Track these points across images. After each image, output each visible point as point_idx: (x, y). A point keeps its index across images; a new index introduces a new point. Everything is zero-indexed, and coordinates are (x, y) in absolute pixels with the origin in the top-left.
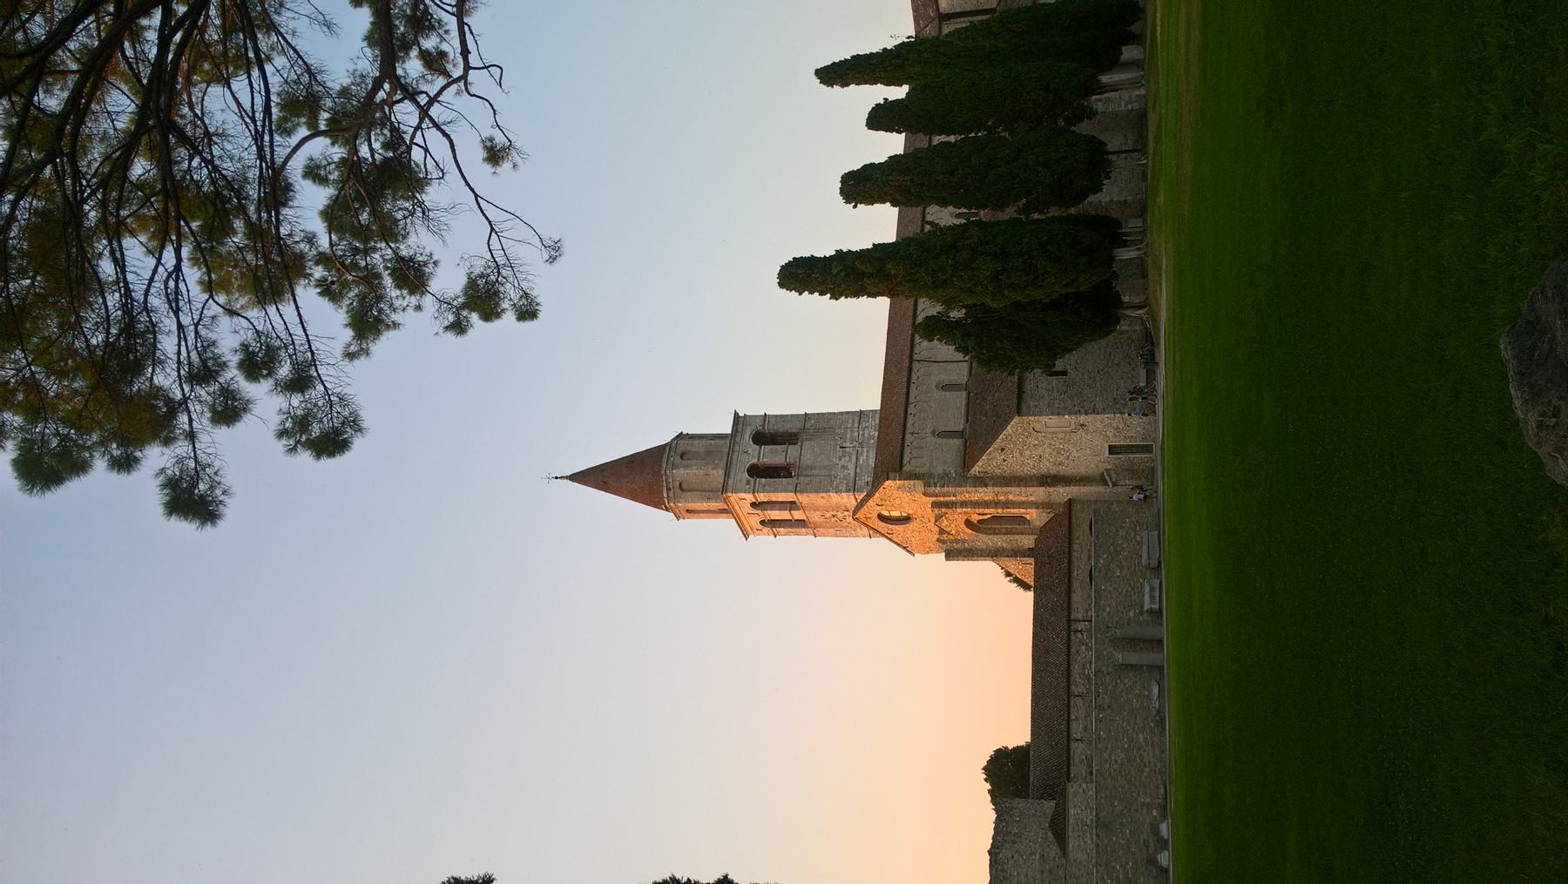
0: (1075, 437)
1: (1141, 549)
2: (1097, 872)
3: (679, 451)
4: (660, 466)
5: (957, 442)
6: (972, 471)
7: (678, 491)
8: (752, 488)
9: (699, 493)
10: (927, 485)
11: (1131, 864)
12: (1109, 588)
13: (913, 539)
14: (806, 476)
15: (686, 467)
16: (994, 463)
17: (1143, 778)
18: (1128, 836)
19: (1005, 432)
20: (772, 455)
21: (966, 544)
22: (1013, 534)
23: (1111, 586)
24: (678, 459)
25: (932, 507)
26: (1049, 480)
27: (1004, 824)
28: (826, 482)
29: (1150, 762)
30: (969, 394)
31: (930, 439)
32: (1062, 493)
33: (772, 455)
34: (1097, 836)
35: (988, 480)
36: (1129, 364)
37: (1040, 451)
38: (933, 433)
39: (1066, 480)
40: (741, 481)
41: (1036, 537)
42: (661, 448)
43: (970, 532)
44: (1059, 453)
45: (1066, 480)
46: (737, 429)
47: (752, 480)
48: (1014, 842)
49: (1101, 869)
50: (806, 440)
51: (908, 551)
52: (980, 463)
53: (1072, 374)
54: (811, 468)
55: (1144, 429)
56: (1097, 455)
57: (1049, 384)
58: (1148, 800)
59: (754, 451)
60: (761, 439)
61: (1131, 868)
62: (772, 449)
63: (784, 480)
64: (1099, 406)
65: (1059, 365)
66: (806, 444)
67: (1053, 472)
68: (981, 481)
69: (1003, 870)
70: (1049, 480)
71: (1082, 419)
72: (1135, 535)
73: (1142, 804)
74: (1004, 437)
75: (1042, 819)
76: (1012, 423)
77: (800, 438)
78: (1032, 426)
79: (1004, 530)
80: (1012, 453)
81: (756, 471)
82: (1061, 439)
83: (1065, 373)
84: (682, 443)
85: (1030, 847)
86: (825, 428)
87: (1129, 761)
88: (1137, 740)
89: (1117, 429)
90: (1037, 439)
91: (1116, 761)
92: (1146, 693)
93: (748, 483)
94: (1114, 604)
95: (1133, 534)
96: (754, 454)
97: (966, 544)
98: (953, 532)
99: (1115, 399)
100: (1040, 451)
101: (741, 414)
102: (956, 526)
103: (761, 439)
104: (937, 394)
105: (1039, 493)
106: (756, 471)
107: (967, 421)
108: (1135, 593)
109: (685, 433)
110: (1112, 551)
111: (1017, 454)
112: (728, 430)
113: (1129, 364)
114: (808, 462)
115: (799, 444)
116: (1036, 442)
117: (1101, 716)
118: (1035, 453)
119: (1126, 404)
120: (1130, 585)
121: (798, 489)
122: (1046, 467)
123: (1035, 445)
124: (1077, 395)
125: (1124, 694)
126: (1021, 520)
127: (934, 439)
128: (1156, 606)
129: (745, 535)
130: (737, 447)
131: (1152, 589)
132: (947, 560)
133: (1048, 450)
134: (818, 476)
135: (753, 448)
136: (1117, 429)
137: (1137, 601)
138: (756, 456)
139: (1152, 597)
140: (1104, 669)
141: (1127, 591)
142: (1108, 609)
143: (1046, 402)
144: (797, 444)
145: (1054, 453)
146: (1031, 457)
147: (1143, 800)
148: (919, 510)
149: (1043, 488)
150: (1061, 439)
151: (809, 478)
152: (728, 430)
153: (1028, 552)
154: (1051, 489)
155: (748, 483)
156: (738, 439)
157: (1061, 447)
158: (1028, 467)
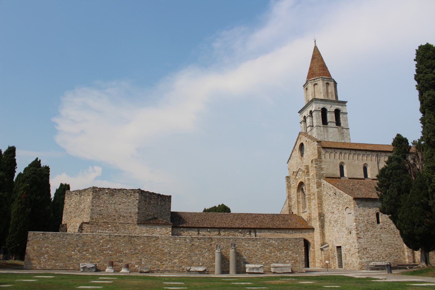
0: (344, 229)
1: (282, 263)
2: (107, 236)
3: (329, 82)
4: (323, 76)
5: (338, 174)
6: (324, 181)
7: (314, 83)
8: (317, 109)
9: (314, 91)
10: (316, 161)
11: (111, 252)
12: (258, 246)
13: (293, 161)
14: (324, 130)
15: (323, 85)
16: (328, 191)
17: (154, 261)
18: (124, 252)
19: (344, 193)
20: (331, 117)
21: (293, 185)
22: (298, 204)
23: (260, 247)
24: (326, 82)
25: (307, 165)
26: (322, 218)
27: (156, 197)
28: (322, 137)
29: (163, 265)
30: (364, 179)
31: (339, 162)
32: (316, 224)
33: (331, 117)
34: (125, 236)
35: (320, 189)
36: (386, 256)
37: (336, 212)
38: (342, 163)
39: (322, 227)
40: (319, 105)
41: (297, 215)
42: (330, 75)
43: (298, 185)
44: (336, 221)
45: (322, 227)
46: (340, 103)
47: (320, 109)
48: (145, 201)
49: (108, 238)
50: (338, 129)
51: (289, 160)
52: (328, 184)
53: (379, 226)
54: (327, 132)
55: (351, 264)
56: (336, 240)
57: (372, 214)
58: (143, 263)
59: (332, 109)
60: (337, 112)
61: (108, 253)
62: (333, 116)
63: (321, 121)
64: (361, 241)
65: (384, 218)
66: (337, 129)
67: (326, 219)
68: (319, 185)
69: (131, 195)
70: (322, 218)
71: (354, 232)
72: (289, 260)
73: (141, 260)
74: (342, 193)
75: (159, 214)
76: (349, 196)
77: (339, 127)
78: (348, 206)
79: (299, 200)
80: (334, 198)
81: (324, 112)
82: (343, 222)
83: (378, 222)
84: (332, 83)
85: (143, 208)
86: (344, 136)
87: (164, 254)
88: (175, 259)
89: (350, 250)
90: (342, 210)
91: (163, 247)
92: (201, 264)
93: (319, 108)
94: (249, 248)
95: (289, 258)
96: (331, 108)
97: (293, 185)
98: (297, 177)
99: (366, 249)
100: (336, 212)
101: (346, 104)
102: (299, 178)
103: (337, 112)
104: (361, 164)
105: (315, 214)
106: (324, 112)
107: (349, 178)
108: (256, 259)
109: (337, 85)
110: (279, 247)
111: (333, 201)
112: (340, 99)
113: (386, 256)
114: (329, 130)
115: (336, 127)
116: (340, 209)
117: (188, 240)
118: (334, 210)
119: (364, 255)
120: (261, 257)
121: (318, 127)
122: (328, 217)
123: (338, 209)
124: (367, 229)
125: (200, 252)
126: (304, 207)
127: (339, 163)
128: (247, 270)
129: (300, 111)
130: (333, 103)
131: (258, 269)
132: (286, 177)
133: (336, 216)
134: (324, 134)
135: (333, 109)
136: (350, 250)
137: (252, 261)
138: (330, 111)
139: (253, 268)
140: (213, 242)
141: (257, 255)
142: (246, 245)
143: (361, 213)
144: (336, 125)
145: (335, 219)
146: (333, 208)
147: (143, 260)
148: (305, 161)
149: (318, 215)
150: (343, 222)
151: (323, 131)
152: (340, 99)
153: (291, 212)
154: (318, 219)
155: (319, 108)
156: (336, 103)
157: (339, 222)
158: (326, 207)
